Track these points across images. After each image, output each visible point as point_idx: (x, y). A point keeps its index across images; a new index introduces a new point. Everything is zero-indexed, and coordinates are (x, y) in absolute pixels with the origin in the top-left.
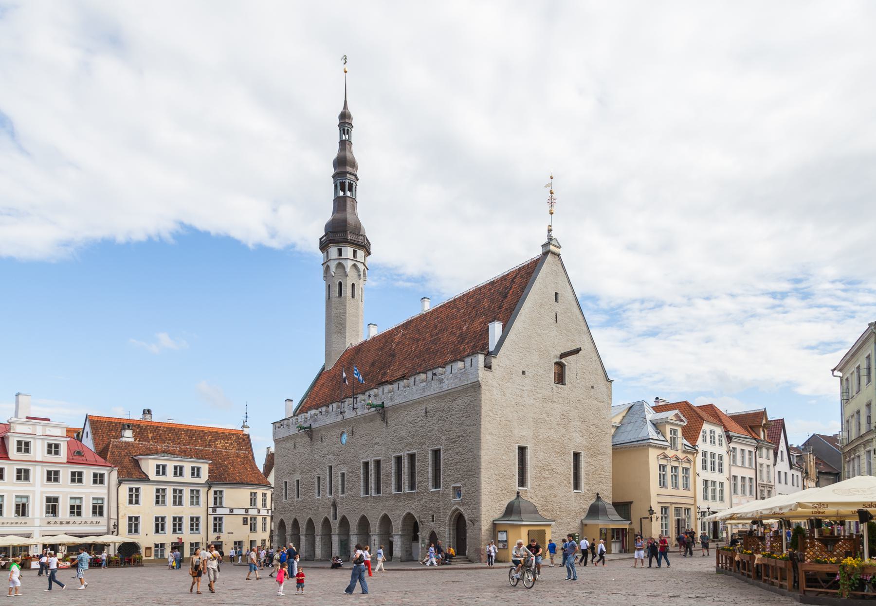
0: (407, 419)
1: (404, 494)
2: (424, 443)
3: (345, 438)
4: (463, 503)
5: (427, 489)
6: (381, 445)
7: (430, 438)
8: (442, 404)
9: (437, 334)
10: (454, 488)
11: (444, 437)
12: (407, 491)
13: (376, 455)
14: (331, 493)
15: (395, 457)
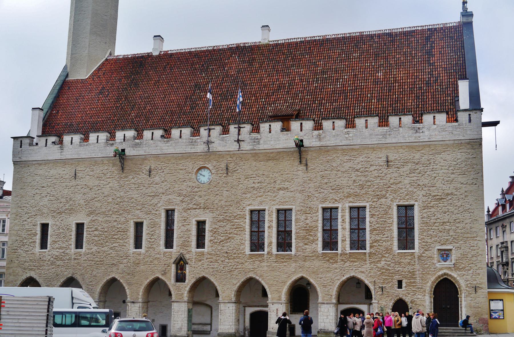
0: (349, 164)
1: (343, 254)
2: (384, 196)
3: (205, 177)
4: (456, 267)
5: (389, 250)
6: (300, 194)
7: (395, 192)
8: (417, 156)
9: (323, 72)
10: (439, 250)
11: (424, 193)
12: (348, 250)
13: (282, 203)
14: (169, 244)
15: (324, 209)
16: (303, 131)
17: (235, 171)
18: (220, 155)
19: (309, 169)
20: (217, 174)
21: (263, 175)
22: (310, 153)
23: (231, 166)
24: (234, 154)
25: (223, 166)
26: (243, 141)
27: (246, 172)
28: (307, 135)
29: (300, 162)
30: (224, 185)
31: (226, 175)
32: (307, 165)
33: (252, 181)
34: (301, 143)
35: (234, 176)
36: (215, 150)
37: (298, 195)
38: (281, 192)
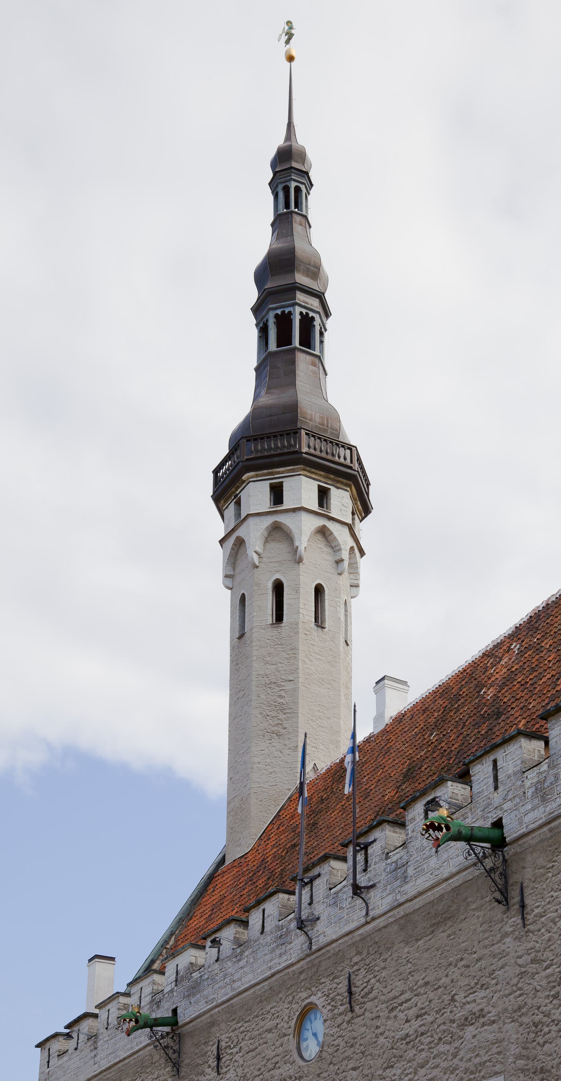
16: (501, 788)
17: (367, 994)
18: (336, 954)
19: (530, 918)
20: (334, 1018)
21: (427, 983)
22: (529, 858)
23: (358, 981)
24: (363, 939)
25: (343, 988)
26: (373, 886)
27: (389, 987)
28: (510, 796)
29: (504, 899)
30: (349, 1052)
31: (350, 1015)
32: (523, 906)
33: (402, 1016)
34: (496, 832)
35: (367, 1014)
36: (323, 940)
37: (511, 1030)
38: (470, 1030)
